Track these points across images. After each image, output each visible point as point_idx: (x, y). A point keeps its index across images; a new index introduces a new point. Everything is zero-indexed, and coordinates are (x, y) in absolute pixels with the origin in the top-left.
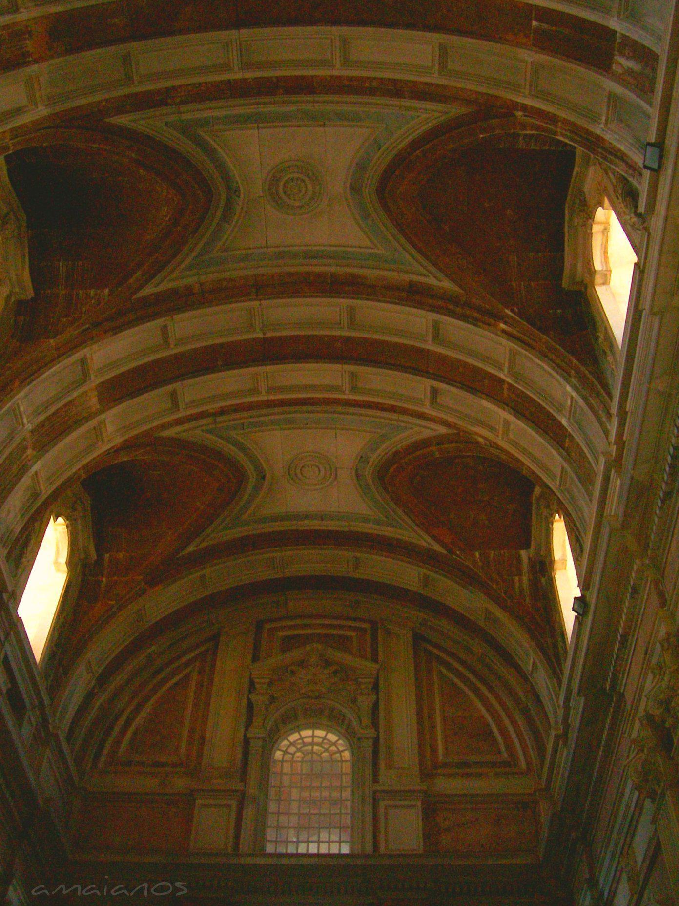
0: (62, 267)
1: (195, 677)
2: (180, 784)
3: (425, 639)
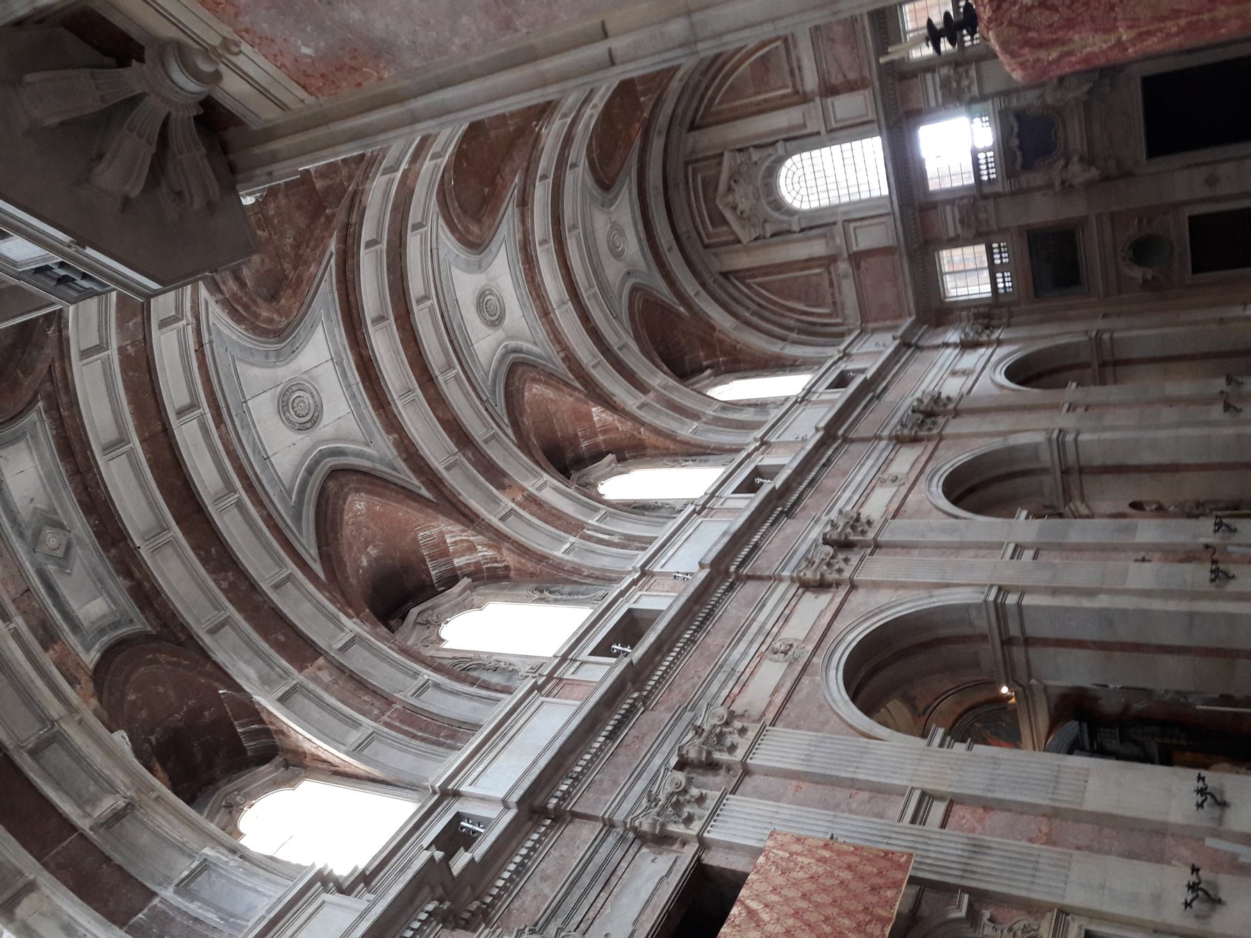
0: (584, 444)
1: (759, 280)
2: (843, 266)
3: (693, 122)
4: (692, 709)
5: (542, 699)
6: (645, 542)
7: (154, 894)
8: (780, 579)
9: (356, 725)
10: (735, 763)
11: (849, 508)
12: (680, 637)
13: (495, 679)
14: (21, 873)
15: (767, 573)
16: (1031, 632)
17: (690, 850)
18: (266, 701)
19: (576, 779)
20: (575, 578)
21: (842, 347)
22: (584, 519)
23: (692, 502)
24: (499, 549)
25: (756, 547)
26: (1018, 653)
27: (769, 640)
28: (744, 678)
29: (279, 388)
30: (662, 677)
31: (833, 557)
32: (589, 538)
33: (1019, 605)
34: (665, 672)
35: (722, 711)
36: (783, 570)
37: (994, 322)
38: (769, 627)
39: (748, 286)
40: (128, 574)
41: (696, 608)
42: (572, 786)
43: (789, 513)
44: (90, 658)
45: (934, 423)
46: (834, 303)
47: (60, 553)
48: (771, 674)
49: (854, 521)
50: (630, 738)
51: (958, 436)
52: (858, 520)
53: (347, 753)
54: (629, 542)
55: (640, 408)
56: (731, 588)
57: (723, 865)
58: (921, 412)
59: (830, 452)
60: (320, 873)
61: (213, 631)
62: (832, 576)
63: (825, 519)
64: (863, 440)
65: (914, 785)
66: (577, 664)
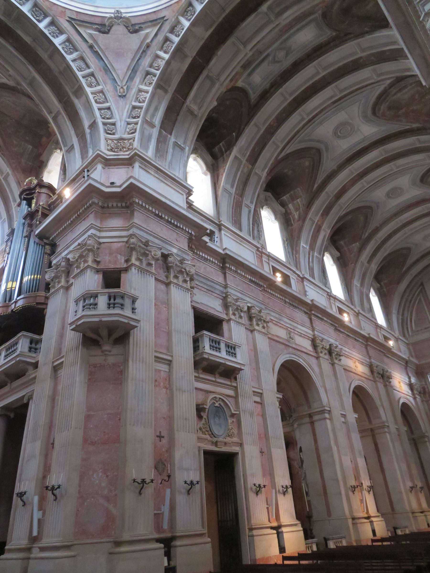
1: (423, 299)
4: (265, 308)
5: (255, 252)
6: (313, 276)
7: (171, 134)
8: (313, 330)
9: (232, 186)
10: (254, 327)
11: (343, 352)
12: (286, 298)
13: (256, 232)
14: (169, 86)
15: (314, 326)
16: (317, 425)
17: (224, 316)
18: (235, 152)
19: (236, 272)
20: (294, 253)
21: (400, 337)
22: (316, 250)
23: (331, 291)
24: (299, 220)
25: (322, 319)
26: (307, 420)
27: (292, 331)
28: (278, 324)
29: (351, 121)
30: (272, 294)
31: (325, 349)
32: (309, 254)
33: (325, 418)
34: (274, 295)
35: (268, 319)
36: (317, 331)
37: (422, 395)
38: (296, 330)
39: (418, 295)
40: (272, 86)
41: (297, 302)
42: (234, 270)
43: (336, 329)
44: (240, 84)
45: (380, 378)
46: (418, 331)
47: (277, 59)
48: (282, 334)
49: (339, 355)
50: (251, 287)
51: (377, 388)
52: (340, 356)
53: (223, 186)
54: (311, 270)
55: (361, 261)
56: (306, 313)
57: (224, 329)
58: (383, 373)
59: (361, 340)
60: (191, 191)
61: (255, 125)
62: (319, 349)
63: (337, 343)
64: (368, 352)
65: (264, 390)
66: (268, 261)
